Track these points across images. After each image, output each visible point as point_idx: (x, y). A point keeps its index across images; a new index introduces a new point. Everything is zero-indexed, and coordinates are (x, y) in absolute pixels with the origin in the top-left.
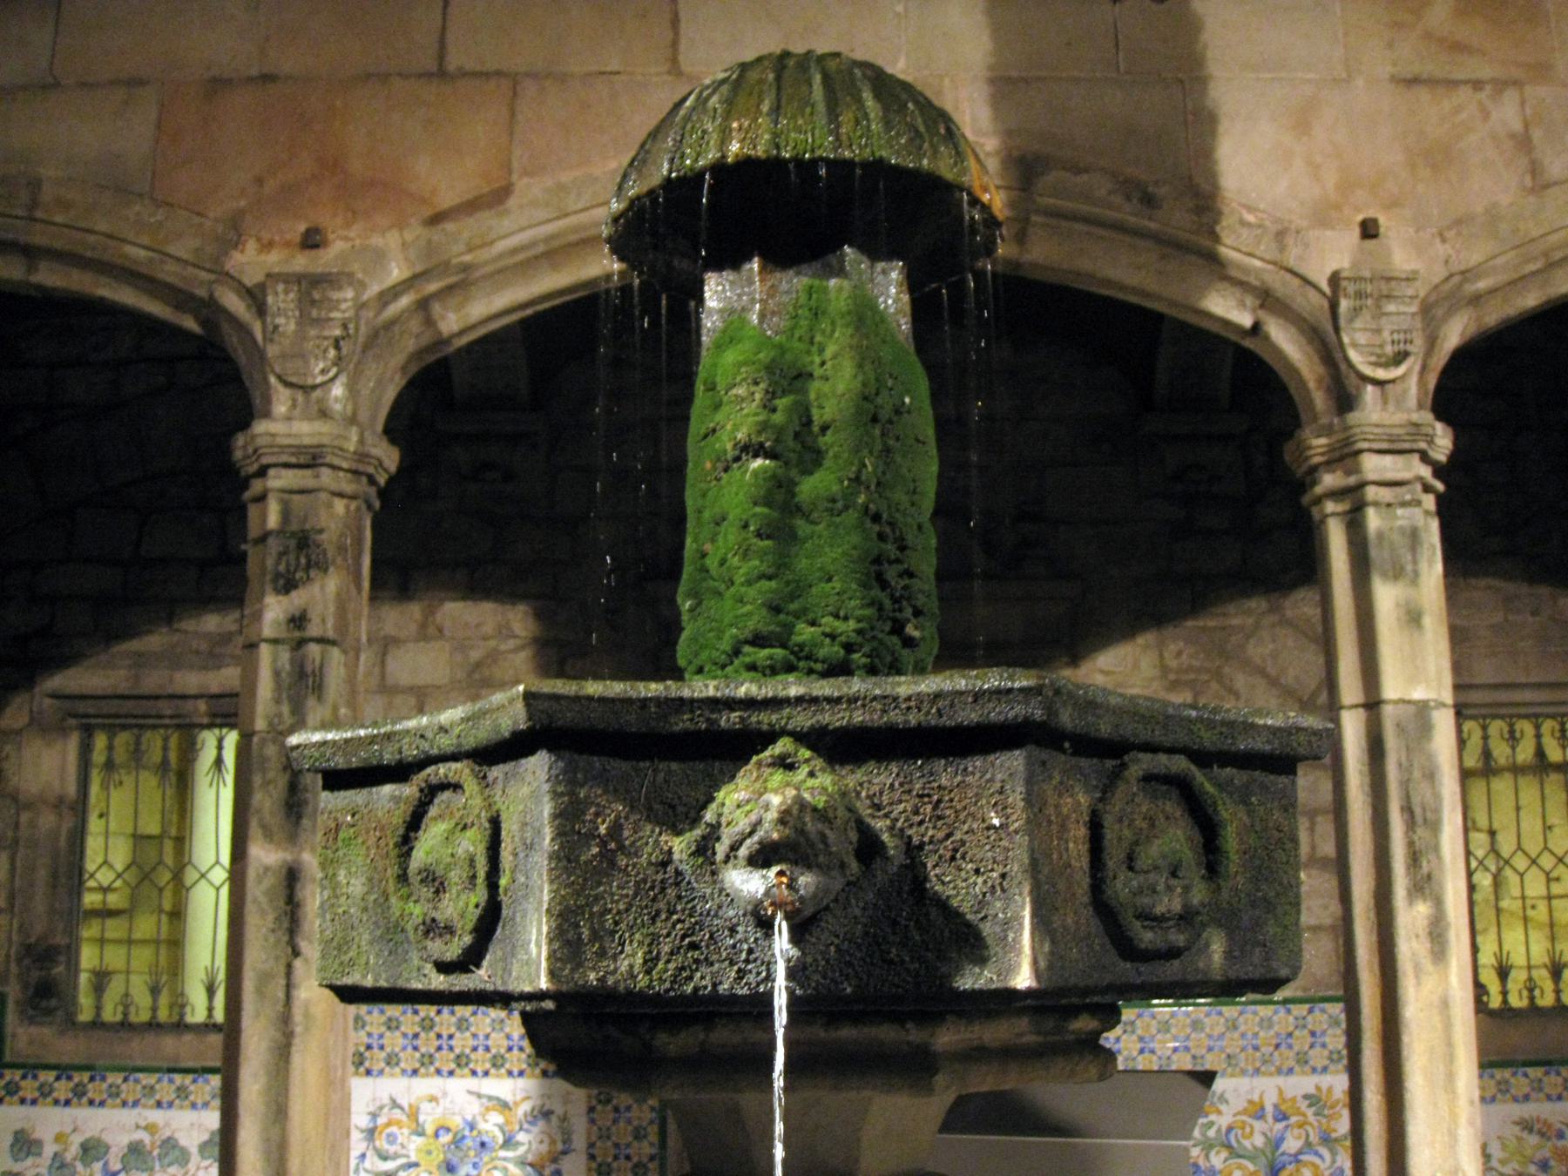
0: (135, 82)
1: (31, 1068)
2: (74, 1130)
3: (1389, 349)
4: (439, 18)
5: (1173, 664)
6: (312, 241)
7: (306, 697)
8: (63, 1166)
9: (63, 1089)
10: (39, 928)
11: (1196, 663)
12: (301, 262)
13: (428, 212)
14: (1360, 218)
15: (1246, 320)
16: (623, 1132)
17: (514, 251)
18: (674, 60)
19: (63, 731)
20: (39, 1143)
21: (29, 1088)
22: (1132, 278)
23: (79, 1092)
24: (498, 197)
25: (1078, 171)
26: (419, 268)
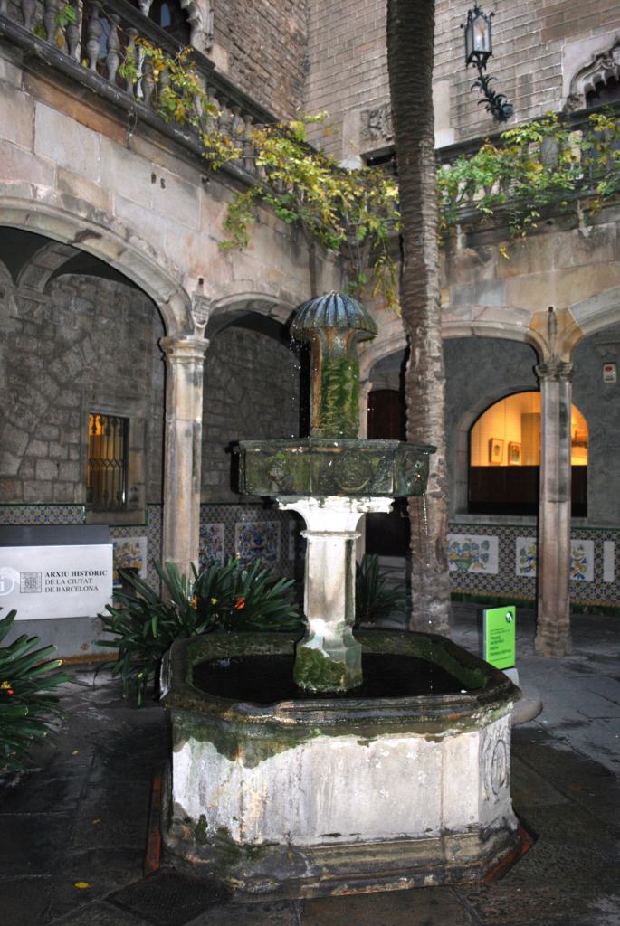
3: (202, 319)
5: (12, 382)
7: (423, 443)
11: (19, 383)
14: (199, 277)
18: (33, 148)
22: (143, 277)
25: (140, 239)
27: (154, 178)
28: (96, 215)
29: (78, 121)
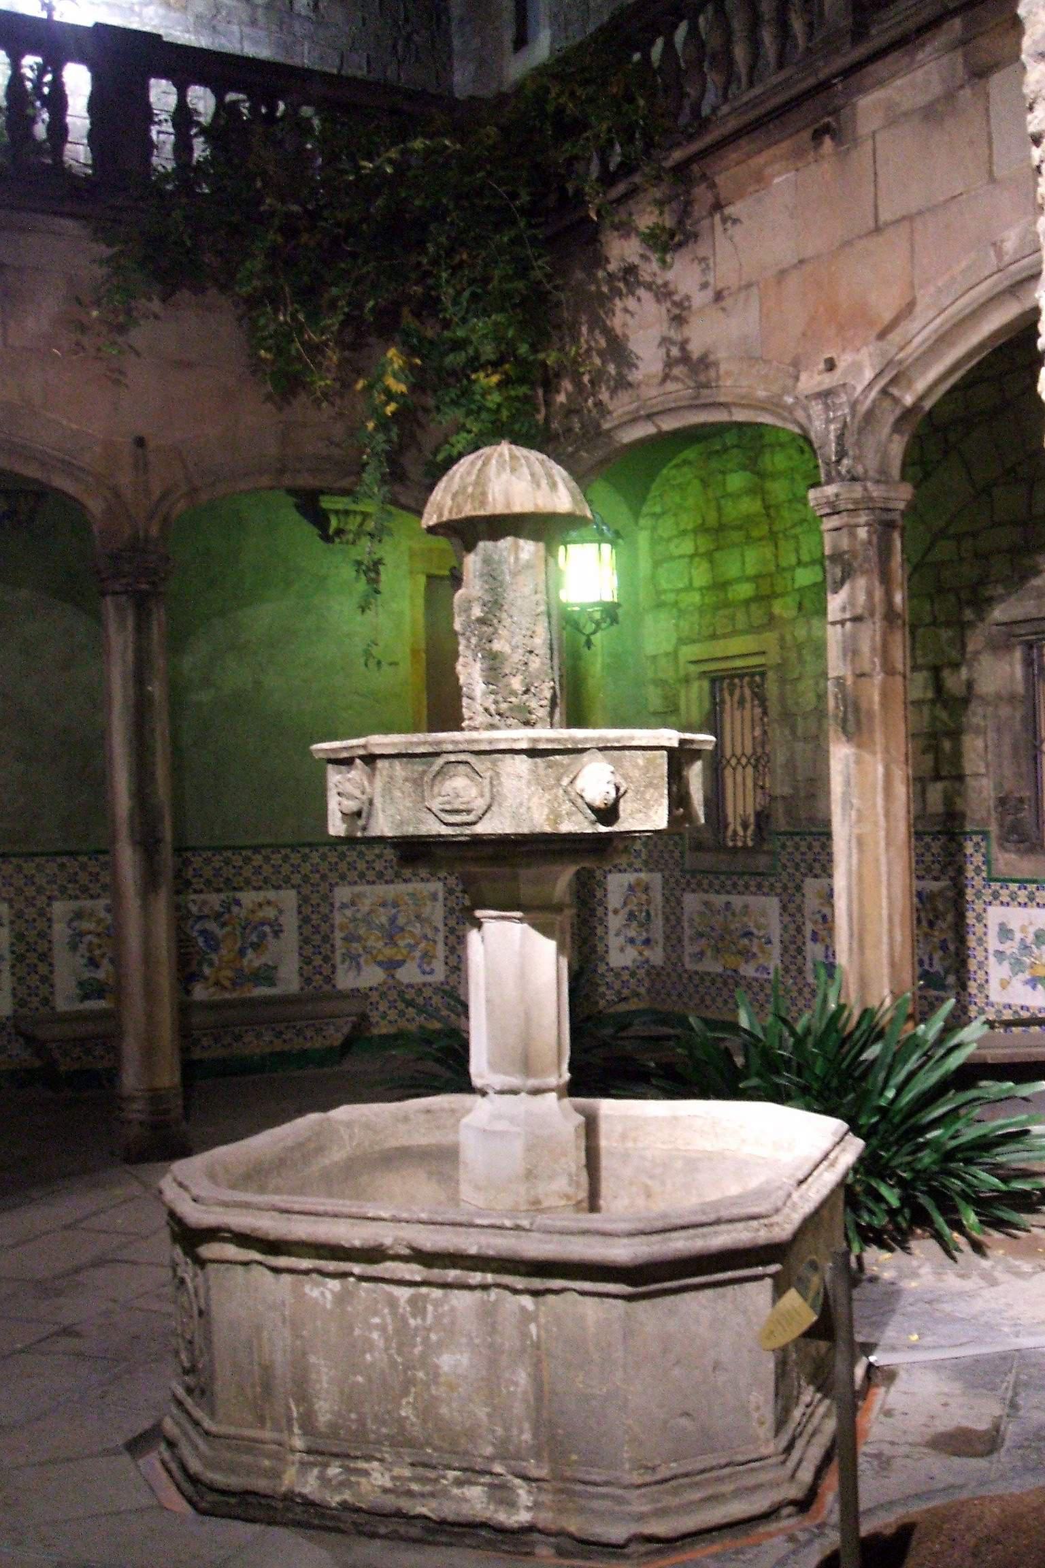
0: (749, 286)
1: (1005, 881)
2: (1031, 924)
4: (872, 189)
6: (831, 365)
8: (1026, 947)
9: (1022, 896)
10: (1007, 786)
12: (828, 380)
13: (878, 329)
17: (924, 342)
18: (990, 172)
19: (1009, 648)
20: (1011, 931)
21: (1005, 895)
23: (1031, 898)
24: (909, 308)
26: (877, 371)
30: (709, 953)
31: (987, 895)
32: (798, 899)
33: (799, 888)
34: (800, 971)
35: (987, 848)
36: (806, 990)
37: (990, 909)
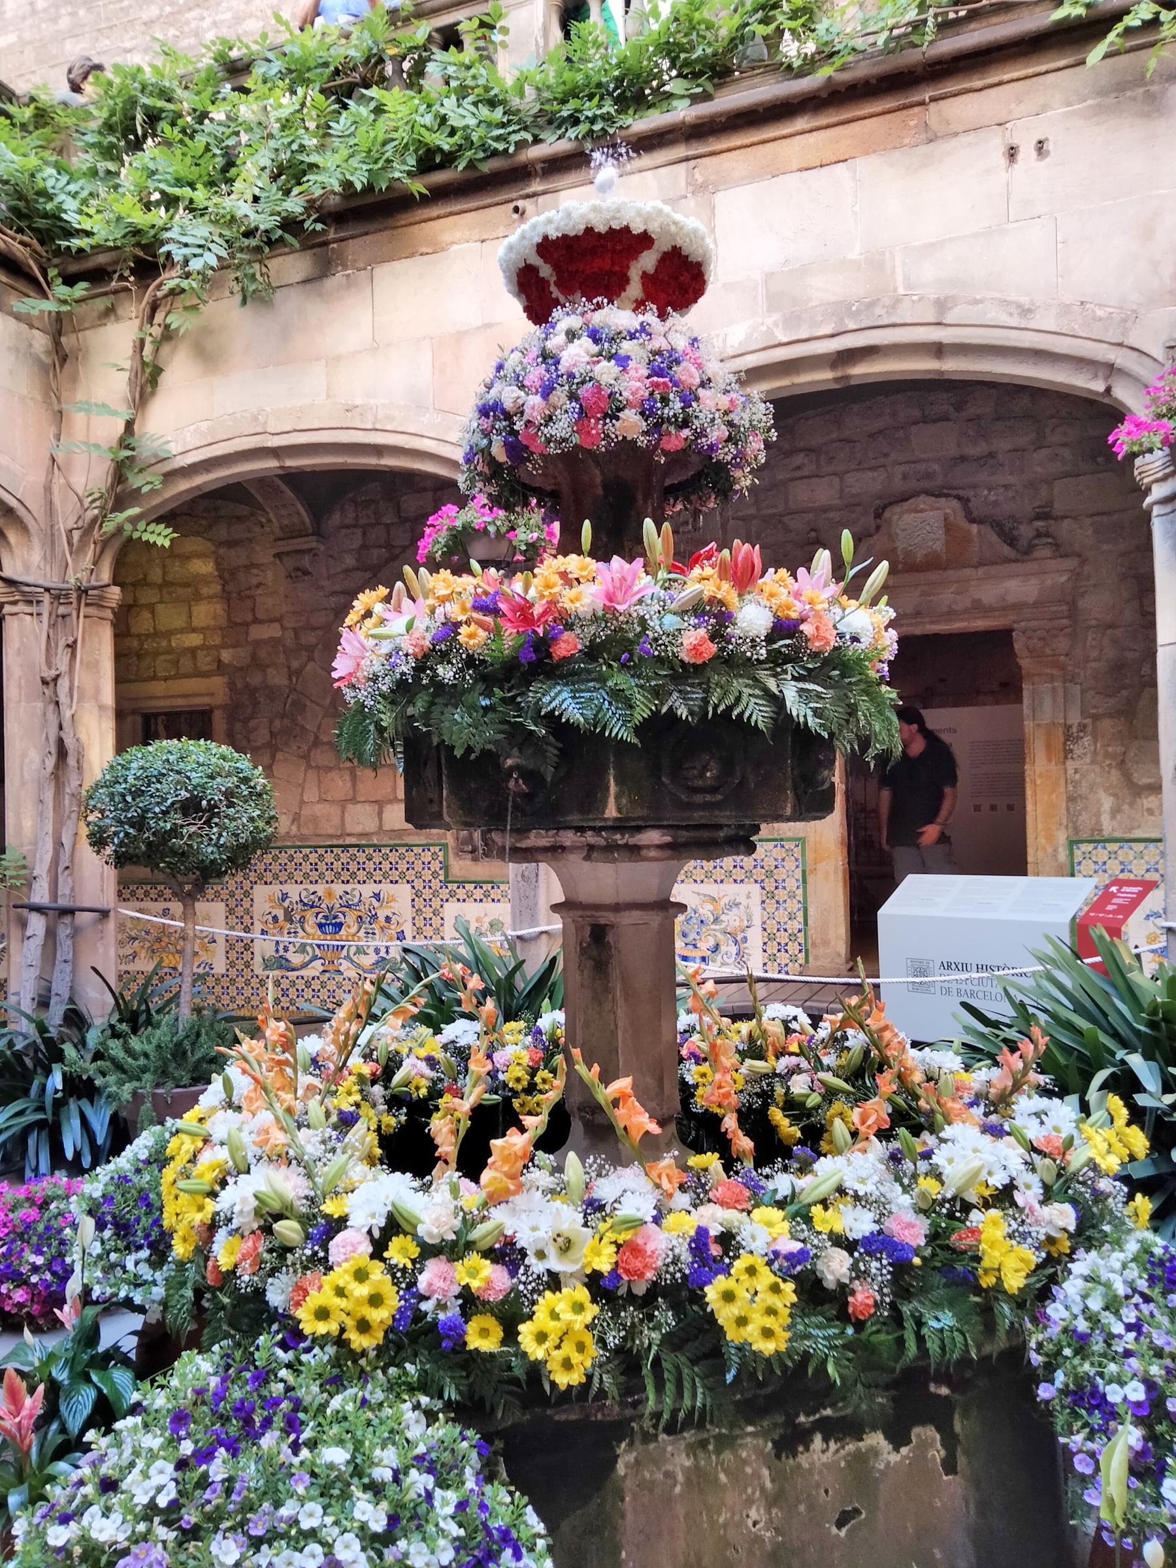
1: (461, 883)
9: (478, 894)
15: (1099, 386)
16: (781, 915)
21: (461, 894)
25: (976, 302)
27: (1012, 153)
28: (855, 315)
29: (800, 170)
30: (143, 954)
31: (444, 894)
32: (246, 903)
33: (247, 894)
34: (247, 965)
35: (446, 856)
36: (254, 981)
37: (446, 905)
